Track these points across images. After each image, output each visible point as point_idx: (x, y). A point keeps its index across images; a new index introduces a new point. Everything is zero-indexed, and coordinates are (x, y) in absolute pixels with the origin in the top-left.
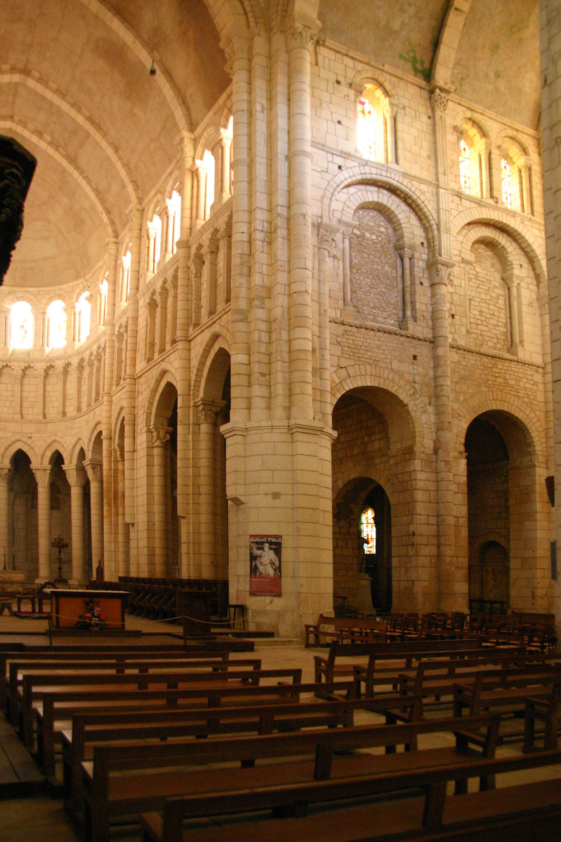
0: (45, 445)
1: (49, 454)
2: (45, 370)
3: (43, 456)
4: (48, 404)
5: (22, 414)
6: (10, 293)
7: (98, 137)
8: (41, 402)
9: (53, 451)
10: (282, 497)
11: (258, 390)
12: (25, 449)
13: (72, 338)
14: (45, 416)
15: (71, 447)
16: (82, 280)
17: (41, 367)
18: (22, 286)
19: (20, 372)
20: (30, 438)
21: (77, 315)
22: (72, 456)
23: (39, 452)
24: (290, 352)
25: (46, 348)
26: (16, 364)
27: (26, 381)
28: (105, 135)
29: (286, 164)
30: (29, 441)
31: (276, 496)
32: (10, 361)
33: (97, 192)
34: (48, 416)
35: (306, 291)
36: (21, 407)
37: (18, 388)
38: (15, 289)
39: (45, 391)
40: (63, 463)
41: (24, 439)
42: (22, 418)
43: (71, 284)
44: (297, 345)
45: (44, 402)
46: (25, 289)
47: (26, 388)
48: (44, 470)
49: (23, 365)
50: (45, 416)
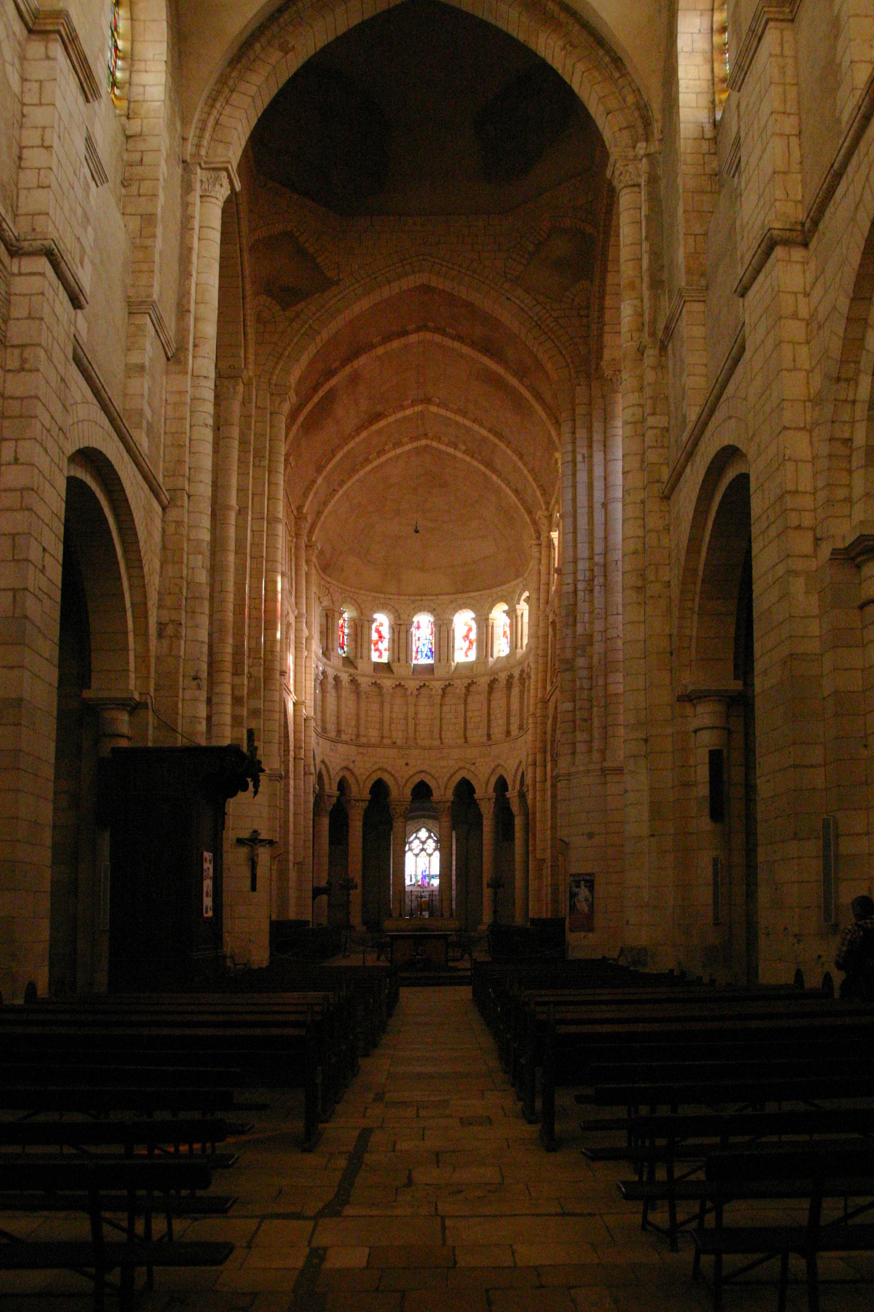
2: (489, 685)
4: (493, 724)
5: (466, 738)
12: (469, 777)
13: (514, 646)
14: (489, 736)
15: (513, 771)
16: (521, 579)
17: (484, 681)
19: (464, 690)
20: (474, 764)
21: (519, 619)
23: (483, 780)
25: (490, 659)
26: (458, 681)
27: (470, 699)
30: (473, 768)
34: (492, 736)
35: (618, 636)
36: (465, 729)
37: (461, 708)
38: (456, 596)
41: (468, 766)
42: (466, 742)
43: (512, 583)
45: (489, 721)
48: (489, 799)
49: (466, 682)
50: (489, 736)
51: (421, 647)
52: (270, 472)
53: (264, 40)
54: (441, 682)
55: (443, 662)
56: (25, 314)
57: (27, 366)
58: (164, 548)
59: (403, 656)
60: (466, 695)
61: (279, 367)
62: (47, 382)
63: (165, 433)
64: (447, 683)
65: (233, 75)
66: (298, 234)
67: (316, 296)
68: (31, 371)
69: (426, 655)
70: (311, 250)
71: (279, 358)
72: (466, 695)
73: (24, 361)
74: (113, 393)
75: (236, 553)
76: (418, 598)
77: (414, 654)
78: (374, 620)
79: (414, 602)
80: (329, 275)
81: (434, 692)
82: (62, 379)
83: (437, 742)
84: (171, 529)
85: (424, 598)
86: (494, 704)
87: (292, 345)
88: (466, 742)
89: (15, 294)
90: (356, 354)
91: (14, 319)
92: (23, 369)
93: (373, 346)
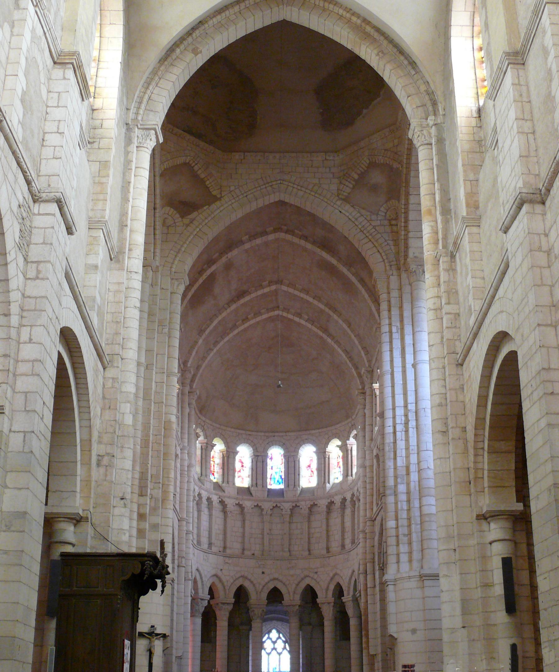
0: (329, 579)
1: (332, 587)
3: (327, 589)
5: (309, 550)
6: (297, 438)
7: (335, 317)
8: (324, 536)
9: (335, 584)
10: (418, 632)
14: (328, 550)
15: (348, 579)
17: (323, 503)
18: (306, 430)
20: (316, 573)
22: (349, 588)
24: (421, 516)
26: (303, 503)
27: (312, 518)
28: (340, 315)
29: (413, 370)
32: (298, 501)
34: (330, 549)
36: (309, 543)
37: (306, 525)
39: (328, 526)
40: (343, 596)
44: (426, 510)
45: (328, 536)
46: (308, 432)
49: (309, 503)
50: (328, 550)
51: (274, 474)
52: (169, 337)
53: (182, 47)
54: (290, 503)
55: (291, 487)
56: (41, 241)
57: (41, 276)
59: (260, 482)
61: (178, 259)
62: (52, 286)
63: (107, 313)
64: (294, 505)
65: (161, 69)
66: (194, 164)
67: (205, 208)
68: (42, 279)
69: (278, 481)
70: (202, 176)
71: (178, 253)
73: (38, 272)
75: (144, 399)
76: (271, 434)
77: (268, 480)
78: (237, 453)
79: (268, 437)
80: (214, 193)
81: (283, 513)
82: (60, 283)
83: (287, 554)
85: (276, 434)
86: (332, 522)
87: (188, 242)
88: (310, 554)
89: (35, 227)
90: (230, 247)
91: (34, 244)
92: (37, 278)
93: (242, 243)
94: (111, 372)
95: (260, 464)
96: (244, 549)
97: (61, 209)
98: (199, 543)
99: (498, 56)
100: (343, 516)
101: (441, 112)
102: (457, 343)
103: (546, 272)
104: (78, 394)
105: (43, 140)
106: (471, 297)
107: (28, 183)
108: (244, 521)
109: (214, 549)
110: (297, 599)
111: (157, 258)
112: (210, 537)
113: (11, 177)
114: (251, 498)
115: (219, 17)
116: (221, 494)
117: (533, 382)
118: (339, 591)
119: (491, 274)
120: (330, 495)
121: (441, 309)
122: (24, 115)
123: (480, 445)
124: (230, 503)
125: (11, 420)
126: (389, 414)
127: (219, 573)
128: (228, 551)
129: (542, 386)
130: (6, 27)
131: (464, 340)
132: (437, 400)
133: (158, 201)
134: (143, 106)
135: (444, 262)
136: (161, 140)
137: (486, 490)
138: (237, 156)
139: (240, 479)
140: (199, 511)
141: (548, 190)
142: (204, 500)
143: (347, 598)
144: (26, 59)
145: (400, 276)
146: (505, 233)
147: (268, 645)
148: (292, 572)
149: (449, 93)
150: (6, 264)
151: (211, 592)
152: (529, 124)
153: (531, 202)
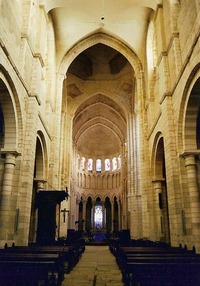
11: (132, 188)
17: (111, 175)
23: (112, 197)
24: (137, 180)
28: (116, 125)
31: (135, 211)
33: (117, 134)
44: (138, 178)
47: (109, 180)
55: (103, 170)
57: (31, 117)
58: (51, 149)
60: (108, 178)
72: (108, 178)
73: (30, 116)
74: (43, 119)
80: (81, 92)
83: (101, 188)
84: (52, 145)
86: (114, 179)
92: (30, 118)
93: (89, 105)
94: (53, 142)
95: (95, 164)
96: (90, 187)
97: (36, 98)
98: (78, 185)
99: (160, 53)
100: (117, 178)
101: (144, 69)
102: (147, 134)
103: (172, 116)
104: (44, 148)
105: (31, 79)
106: (151, 121)
107: (27, 91)
108: (90, 179)
109: (82, 187)
110: (104, 200)
111: (66, 110)
112: (81, 184)
113: (22, 90)
114: (92, 173)
115: (81, 42)
116: (84, 172)
117: (167, 147)
118: (115, 198)
119: (157, 116)
120: (113, 173)
121: (143, 124)
122: (25, 72)
123: (153, 162)
124: (87, 175)
125: (23, 157)
126: (129, 152)
127: (84, 193)
128: (86, 187)
129: (170, 148)
130: (19, 46)
131: (149, 133)
132: (142, 149)
133: (66, 94)
134: (61, 68)
135: (144, 111)
136: (66, 78)
137: (155, 174)
138: (87, 81)
139: (89, 168)
140: (78, 177)
141: (173, 92)
142: (80, 174)
143: (117, 200)
144: (25, 56)
145: (132, 115)
146: (161, 104)
147: (97, 211)
148: (103, 193)
149: (146, 64)
150: (21, 114)
151: (81, 198)
152: (168, 73)
153: (168, 96)
